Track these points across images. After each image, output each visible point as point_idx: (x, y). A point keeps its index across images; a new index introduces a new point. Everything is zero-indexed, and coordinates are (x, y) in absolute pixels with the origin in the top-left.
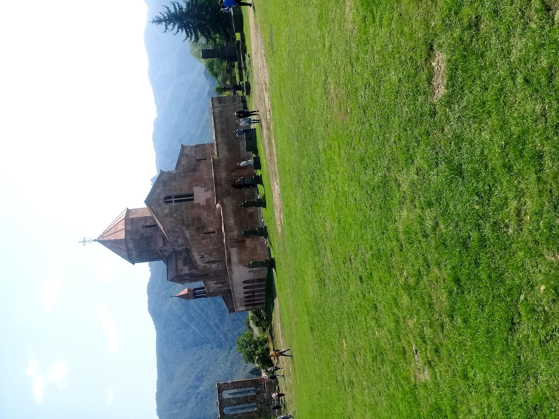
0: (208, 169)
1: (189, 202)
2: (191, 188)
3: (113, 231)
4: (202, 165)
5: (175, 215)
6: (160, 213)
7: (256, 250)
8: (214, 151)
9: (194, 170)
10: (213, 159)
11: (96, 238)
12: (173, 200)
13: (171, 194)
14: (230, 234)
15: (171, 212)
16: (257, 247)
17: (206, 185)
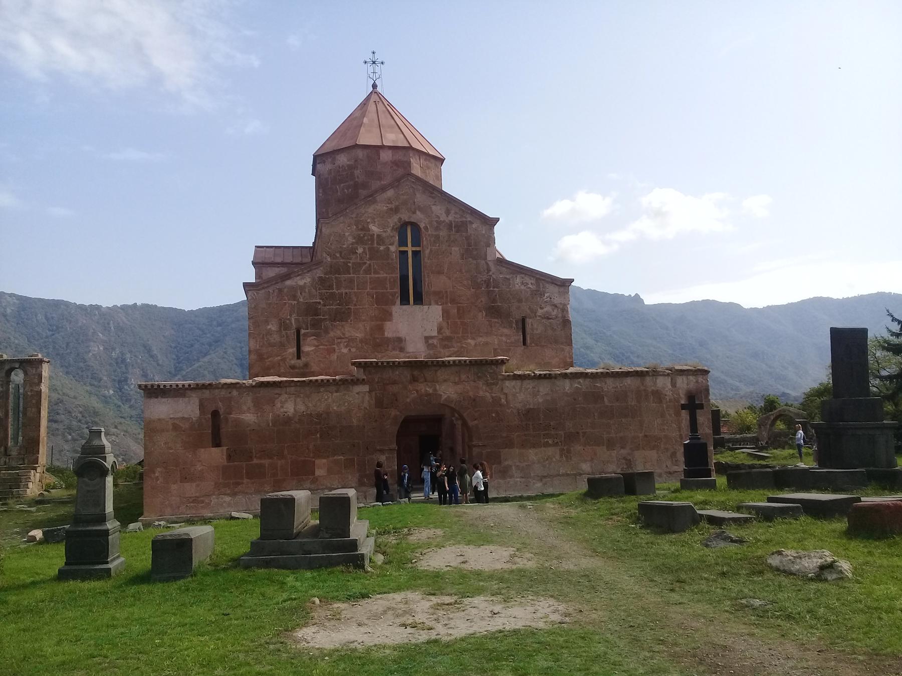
0: (495, 350)
1: (397, 290)
2: (440, 297)
4: (507, 334)
5: (360, 251)
6: (371, 209)
7: (185, 479)
8: (532, 367)
9: (495, 312)
10: (502, 361)
11: (379, 89)
12: (410, 249)
13: (425, 243)
14: (248, 401)
16: (195, 484)
17: (446, 341)
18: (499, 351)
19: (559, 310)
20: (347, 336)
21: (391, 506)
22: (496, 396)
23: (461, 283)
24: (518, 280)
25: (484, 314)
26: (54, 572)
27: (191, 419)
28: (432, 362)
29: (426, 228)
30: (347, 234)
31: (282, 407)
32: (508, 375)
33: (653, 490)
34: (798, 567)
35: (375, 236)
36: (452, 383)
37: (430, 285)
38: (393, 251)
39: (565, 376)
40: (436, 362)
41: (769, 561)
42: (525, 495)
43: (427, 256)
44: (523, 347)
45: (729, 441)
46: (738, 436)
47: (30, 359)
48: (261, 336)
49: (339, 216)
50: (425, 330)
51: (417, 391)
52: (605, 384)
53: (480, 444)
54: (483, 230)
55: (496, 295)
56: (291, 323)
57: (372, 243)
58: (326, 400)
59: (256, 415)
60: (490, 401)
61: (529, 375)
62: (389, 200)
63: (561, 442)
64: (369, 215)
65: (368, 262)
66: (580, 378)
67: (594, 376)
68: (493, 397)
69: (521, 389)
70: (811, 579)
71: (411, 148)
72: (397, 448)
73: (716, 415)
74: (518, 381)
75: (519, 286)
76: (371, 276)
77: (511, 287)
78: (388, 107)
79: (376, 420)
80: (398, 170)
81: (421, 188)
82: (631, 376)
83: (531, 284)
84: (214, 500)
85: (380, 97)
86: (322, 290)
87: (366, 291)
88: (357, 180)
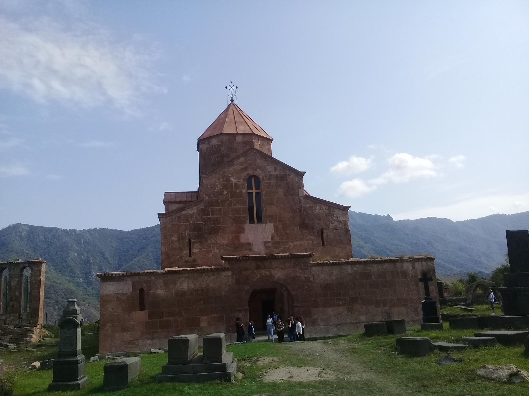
0: (306, 249)
1: (247, 215)
2: (272, 218)
3: (238, 119)
4: (312, 239)
6: (231, 169)
7: (124, 329)
8: (328, 258)
9: (305, 226)
10: (310, 256)
11: (234, 102)
12: (254, 191)
13: (262, 187)
14: (160, 282)
15: (232, 186)
17: (276, 244)
18: (308, 249)
19: (343, 224)
20: (218, 242)
21: (246, 344)
22: (307, 276)
23: (284, 210)
24: (318, 207)
25: (299, 227)
26: (46, 386)
27: (127, 294)
28: (269, 256)
29: (263, 179)
30: (217, 183)
31: (181, 286)
32: (314, 264)
33: (405, 331)
34: (496, 375)
35: (234, 184)
36: (281, 269)
37: (266, 211)
38: (244, 192)
39: (348, 263)
40: (270, 256)
41: (479, 372)
42: (327, 336)
43: (264, 195)
44: (322, 247)
45: (449, 301)
46: (454, 298)
47: (35, 261)
48: (168, 243)
49: (213, 173)
50: (264, 238)
51: (260, 274)
52: (373, 267)
53: (299, 306)
54: (297, 179)
55: (305, 217)
56: (186, 236)
57: (232, 189)
58: (207, 281)
59: (165, 290)
60: (304, 279)
61: (326, 263)
62: (241, 163)
63: (347, 303)
64: (230, 172)
65: (230, 199)
66: (356, 264)
67: (365, 263)
68: (305, 277)
69: (322, 272)
70: (505, 383)
71: (253, 134)
72: (249, 309)
73: (440, 285)
74: (320, 267)
75: (319, 211)
76: (232, 207)
77: (314, 211)
78: (240, 112)
79: (236, 292)
80: (246, 146)
81: (259, 156)
82: (388, 263)
83: (326, 209)
84: (141, 343)
85: (235, 107)
86: (203, 216)
87: (229, 216)
88: (223, 153)
